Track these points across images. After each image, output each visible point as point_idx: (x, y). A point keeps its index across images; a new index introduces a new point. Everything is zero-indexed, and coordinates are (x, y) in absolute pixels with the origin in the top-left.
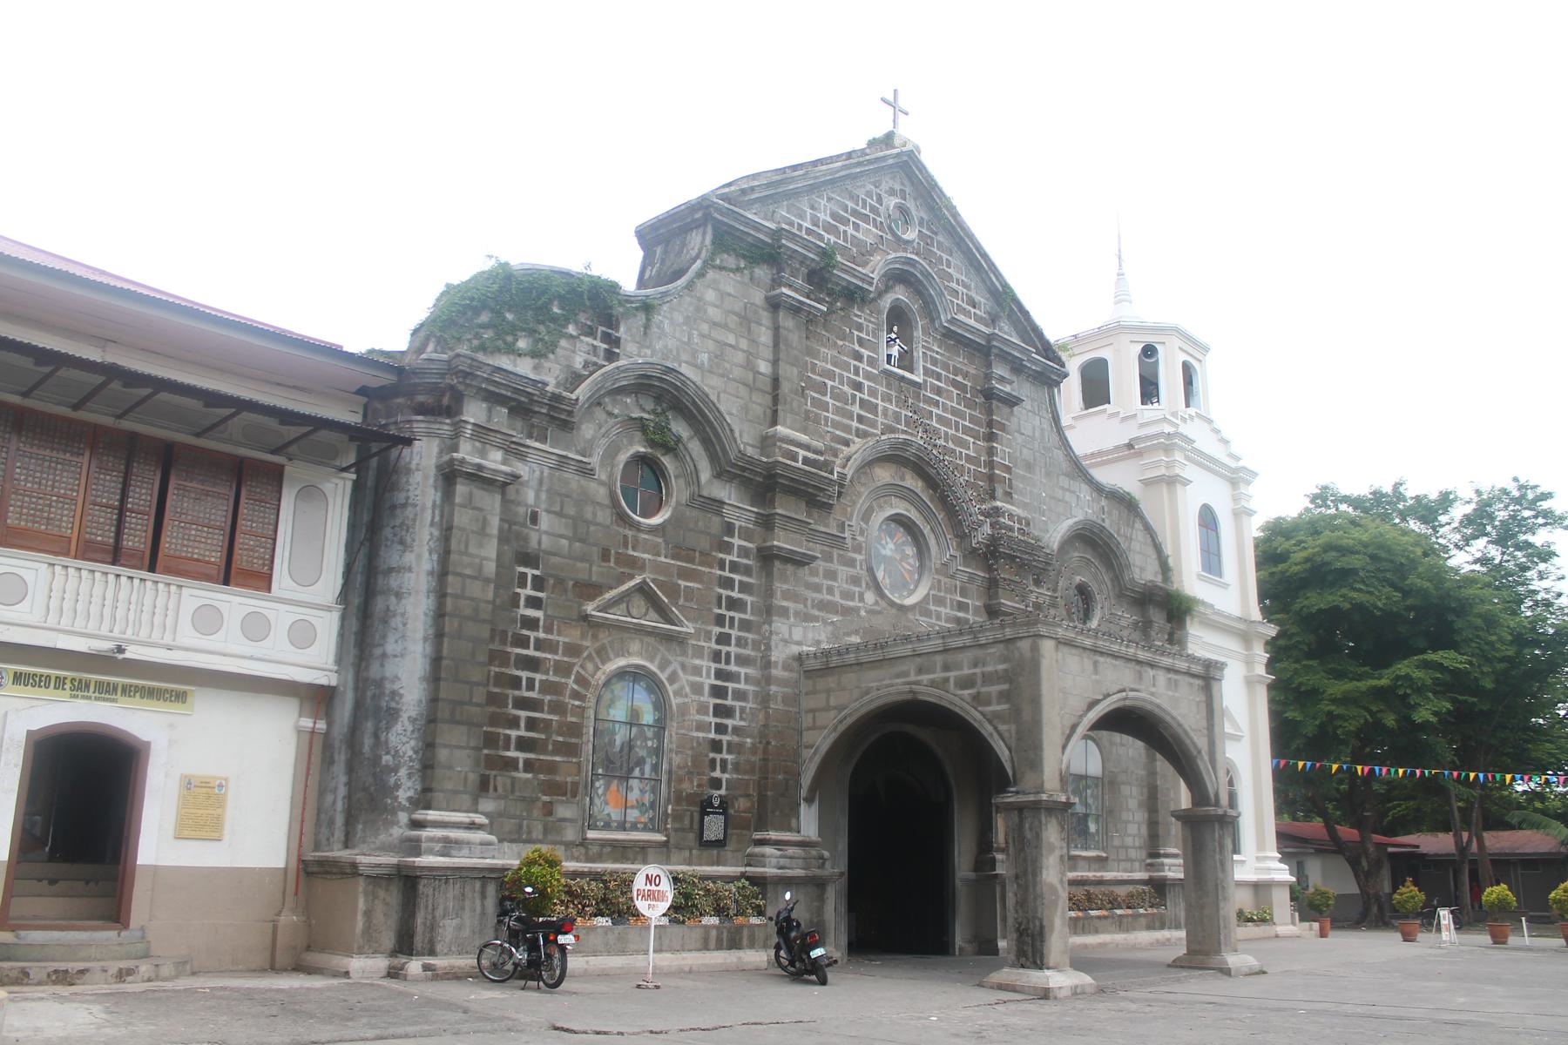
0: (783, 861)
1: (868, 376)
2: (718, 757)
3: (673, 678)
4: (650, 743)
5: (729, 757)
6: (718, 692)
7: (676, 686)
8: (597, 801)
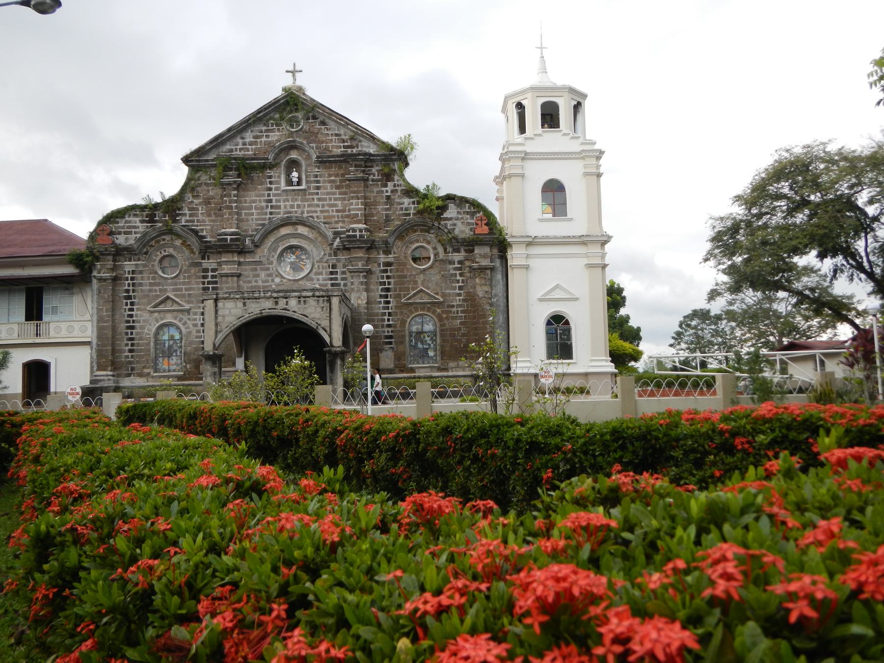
1: (275, 195)
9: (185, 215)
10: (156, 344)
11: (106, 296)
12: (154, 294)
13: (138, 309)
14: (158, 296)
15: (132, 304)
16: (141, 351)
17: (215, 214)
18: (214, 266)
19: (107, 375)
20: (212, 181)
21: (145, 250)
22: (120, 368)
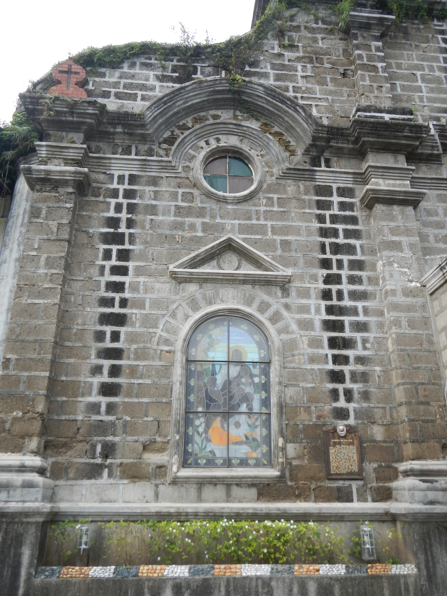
0: (431, 495)
2: (340, 387)
3: (275, 318)
4: (256, 380)
5: (355, 387)
6: (330, 326)
7: (280, 325)
8: (197, 438)
9: (265, 75)
10: (188, 374)
11: (53, 225)
12: (188, 235)
13: (139, 271)
14: (198, 241)
15: (124, 255)
16: (141, 391)
17: (333, 80)
18: (346, 182)
19: (22, 469)
20: (320, 25)
21: (167, 134)
22: (66, 446)
